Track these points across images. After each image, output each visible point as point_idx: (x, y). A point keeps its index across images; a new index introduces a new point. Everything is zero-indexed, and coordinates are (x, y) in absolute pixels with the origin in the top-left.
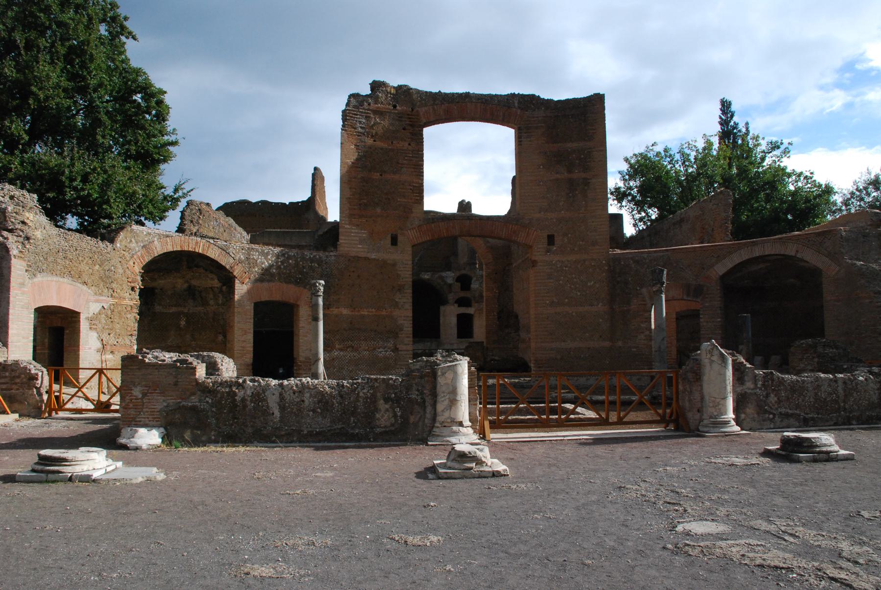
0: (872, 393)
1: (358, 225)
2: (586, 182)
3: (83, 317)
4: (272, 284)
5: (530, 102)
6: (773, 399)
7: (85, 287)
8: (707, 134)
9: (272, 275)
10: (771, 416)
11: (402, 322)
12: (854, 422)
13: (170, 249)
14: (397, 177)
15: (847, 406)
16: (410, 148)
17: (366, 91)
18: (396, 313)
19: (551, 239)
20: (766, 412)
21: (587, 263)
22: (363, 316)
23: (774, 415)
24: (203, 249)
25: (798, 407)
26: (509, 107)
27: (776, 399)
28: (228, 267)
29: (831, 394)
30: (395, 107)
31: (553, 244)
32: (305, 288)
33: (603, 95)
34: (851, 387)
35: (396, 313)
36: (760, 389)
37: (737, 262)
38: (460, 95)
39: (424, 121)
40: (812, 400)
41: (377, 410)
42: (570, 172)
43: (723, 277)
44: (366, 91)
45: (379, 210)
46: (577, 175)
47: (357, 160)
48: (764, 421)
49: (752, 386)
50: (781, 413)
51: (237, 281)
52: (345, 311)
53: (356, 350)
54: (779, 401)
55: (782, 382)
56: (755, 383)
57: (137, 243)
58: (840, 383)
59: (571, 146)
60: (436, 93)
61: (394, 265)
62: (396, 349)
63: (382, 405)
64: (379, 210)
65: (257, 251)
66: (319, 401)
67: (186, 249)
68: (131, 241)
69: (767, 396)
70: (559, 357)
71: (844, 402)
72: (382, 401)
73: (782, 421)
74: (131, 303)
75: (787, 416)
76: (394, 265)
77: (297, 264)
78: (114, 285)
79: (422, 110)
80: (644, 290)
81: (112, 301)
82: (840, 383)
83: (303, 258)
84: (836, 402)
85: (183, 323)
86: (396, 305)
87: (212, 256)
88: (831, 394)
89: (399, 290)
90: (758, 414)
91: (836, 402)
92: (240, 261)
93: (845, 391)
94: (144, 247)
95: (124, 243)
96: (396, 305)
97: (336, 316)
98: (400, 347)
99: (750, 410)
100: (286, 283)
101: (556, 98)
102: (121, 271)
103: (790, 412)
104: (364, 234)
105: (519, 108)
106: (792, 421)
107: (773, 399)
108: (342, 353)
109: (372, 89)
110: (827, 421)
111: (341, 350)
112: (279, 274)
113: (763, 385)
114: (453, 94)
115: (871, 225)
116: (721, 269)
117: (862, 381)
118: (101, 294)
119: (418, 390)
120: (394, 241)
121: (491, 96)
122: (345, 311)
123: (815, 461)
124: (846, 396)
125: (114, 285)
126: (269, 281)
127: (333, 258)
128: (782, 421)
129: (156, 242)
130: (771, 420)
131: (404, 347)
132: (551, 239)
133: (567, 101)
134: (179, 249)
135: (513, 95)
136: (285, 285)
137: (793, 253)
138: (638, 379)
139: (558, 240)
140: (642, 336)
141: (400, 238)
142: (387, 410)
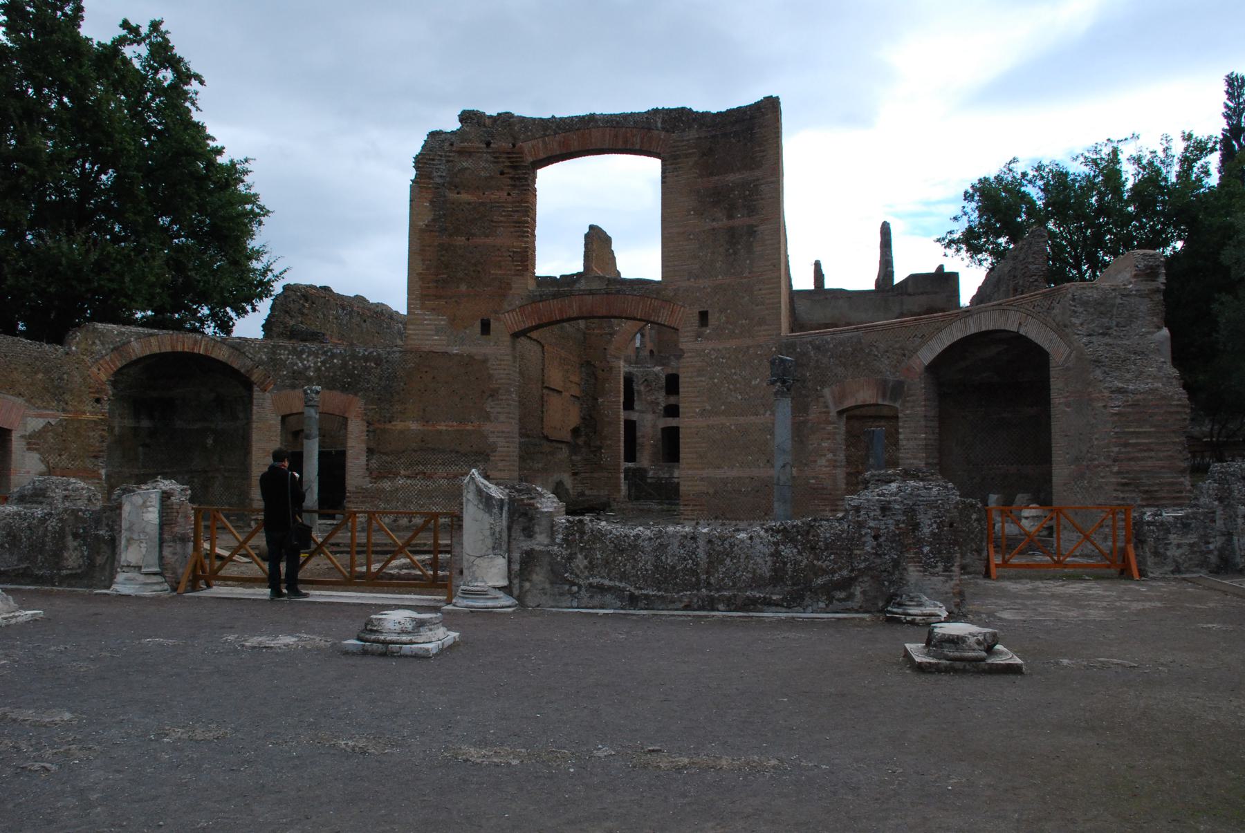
0: (759, 560)
2: (751, 231)
3: (15, 436)
5: (679, 119)
6: (581, 561)
7: (20, 401)
8: (1115, 138)
10: (575, 589)
12: (721, 607)
13: (156, 350)
14: (490, 241)
15: (712, 580)
17: (453, 125)
18: (488, 427)
19: (704, 316)
20: (566, 581)
21: (751, 351)
23: (580, 587)
24: (206, 349)
25: (623, 577)
26: (650, 129)
27: (586, 562)
29: (685, 559)
30: (488, 144)
31: (706, 325)
32: (356, 394)
33: (777, 98)
34: (720, 552)
35: (488, 427)
36: (560, 545)
37: (947, 343)
38: (581, 119)
39: (530, 159)
40: (649, 566)
41: (65, 548)
42: (730, 217)
43: (934, 368)
44: (453, 125)
45: (463, 288)
46: (740, 220)
47: (433, 220)
48: (561, 594)
49: (546, 541)
50: (590, 584)
51: (256, 388)
52: (414, 426)
53: (430, 477)
54: (591, 567)
55: (599, 536)
56: (552, 534)
57: (103, 344)
58: (701, 543)
59: (733, 178)
61: (485, 361)
63: (71, 542)
64: (463, 288)
65: (285, 348)
66: (8, 534)
67: (180, 349)
68: (94, 343)
69: (571, 558)
70: (711, 491)
71: (707, 573)
72: (70, 538)
73: (591, 597)
74: (95, 418)
75: (602, 589)
76: (485, 361)
77: (345, 365)
78: (67, 397)
79: (526, 146)
80: (827, 392)
81: (63, 416)
82: (701, 543)
83: (354, 356)
84: (694, 572)
85: (210, 441)
86: (487, 417)
87: (221, 358)
88: (685, 559)
89: (492, 396)
90: (552, 583)
91: (694, 572)
92: (261, 363)
93: (709, 555)
94: (115, 349)
95: (83, 346)
96: (487, 417)
97: (401, 432)
99: (539, 577)
101: (714, 110)
102: (78, 379)
103: (607, 582)
104: (443, 321)
105: (663, 129)
106: (609, 598)
107: (581, 561)
108: (409, 482)
109: (461, 121)
110: (672, 601)
111: (408, 477)
112: (319, 377)
113: (565, 540)
114: (571, 119)
115: (1135, 276)
116: (927, 355)
117: (742, 541)
118: (45, 408)
119: (107, 525)
120: (486, 327)
121: (625, 117)
122: (414, 426)
123: (365, 653)
124: (710, 563)
125: (67, 397)
127: (398, 354)
128: (591, 597)
129: (134, 344)
130: (573, 595)
132: (704, 316)
133: (730, 112)
134: (169, 349)
135: (656, 111)
137: (1014, 329)
139: (712, 320)
140: (823, 461)
141: (493, 325)
142: (76, 549)
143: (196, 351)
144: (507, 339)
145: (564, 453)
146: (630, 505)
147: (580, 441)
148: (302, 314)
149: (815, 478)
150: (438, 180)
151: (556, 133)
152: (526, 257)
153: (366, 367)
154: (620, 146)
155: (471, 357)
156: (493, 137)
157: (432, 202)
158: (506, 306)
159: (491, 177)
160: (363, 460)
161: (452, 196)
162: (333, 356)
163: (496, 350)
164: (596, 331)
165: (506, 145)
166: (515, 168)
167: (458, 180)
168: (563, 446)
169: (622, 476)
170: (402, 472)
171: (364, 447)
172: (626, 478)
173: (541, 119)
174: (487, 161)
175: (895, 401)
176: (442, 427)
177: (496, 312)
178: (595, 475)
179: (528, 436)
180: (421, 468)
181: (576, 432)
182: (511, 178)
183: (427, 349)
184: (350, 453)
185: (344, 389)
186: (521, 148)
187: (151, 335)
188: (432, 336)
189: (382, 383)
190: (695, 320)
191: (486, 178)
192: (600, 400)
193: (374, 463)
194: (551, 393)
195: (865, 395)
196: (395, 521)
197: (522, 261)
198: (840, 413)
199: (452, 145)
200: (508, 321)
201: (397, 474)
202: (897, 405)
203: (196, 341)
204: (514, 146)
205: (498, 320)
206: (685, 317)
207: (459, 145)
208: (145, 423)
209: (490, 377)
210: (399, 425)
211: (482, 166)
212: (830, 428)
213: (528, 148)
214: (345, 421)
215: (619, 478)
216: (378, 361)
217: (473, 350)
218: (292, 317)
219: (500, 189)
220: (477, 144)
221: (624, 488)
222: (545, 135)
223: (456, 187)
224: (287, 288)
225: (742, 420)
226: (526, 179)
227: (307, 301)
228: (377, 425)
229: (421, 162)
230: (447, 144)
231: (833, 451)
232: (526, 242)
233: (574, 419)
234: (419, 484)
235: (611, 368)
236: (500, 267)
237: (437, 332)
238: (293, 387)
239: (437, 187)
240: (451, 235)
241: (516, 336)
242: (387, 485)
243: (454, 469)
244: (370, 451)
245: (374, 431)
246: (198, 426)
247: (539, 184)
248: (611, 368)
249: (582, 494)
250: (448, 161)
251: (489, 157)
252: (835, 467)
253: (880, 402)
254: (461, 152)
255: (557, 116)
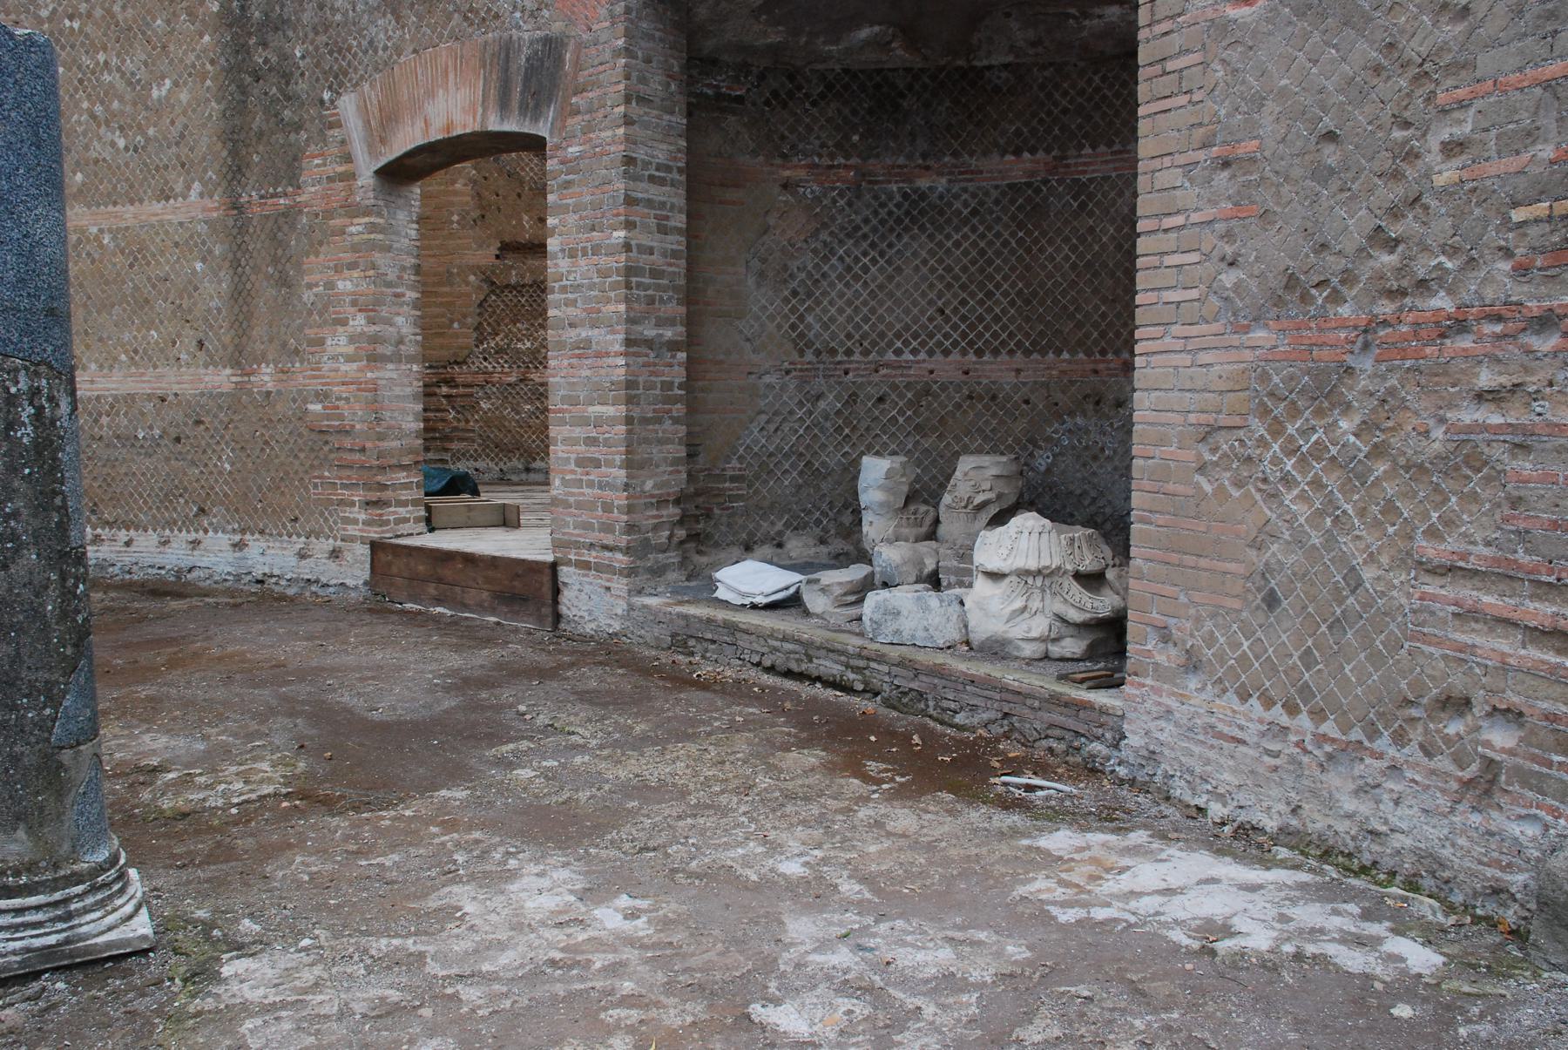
80: (348, 105)
138: (335, 554)
149: (322, 396)
175: (535, 119)
195: (453, 107)
198: (397, 174)
202: (542, 129)
212: (357, 227)
225: (128, 214)
231: (369, 308)
252: (374, 359)
253: (495, 124)
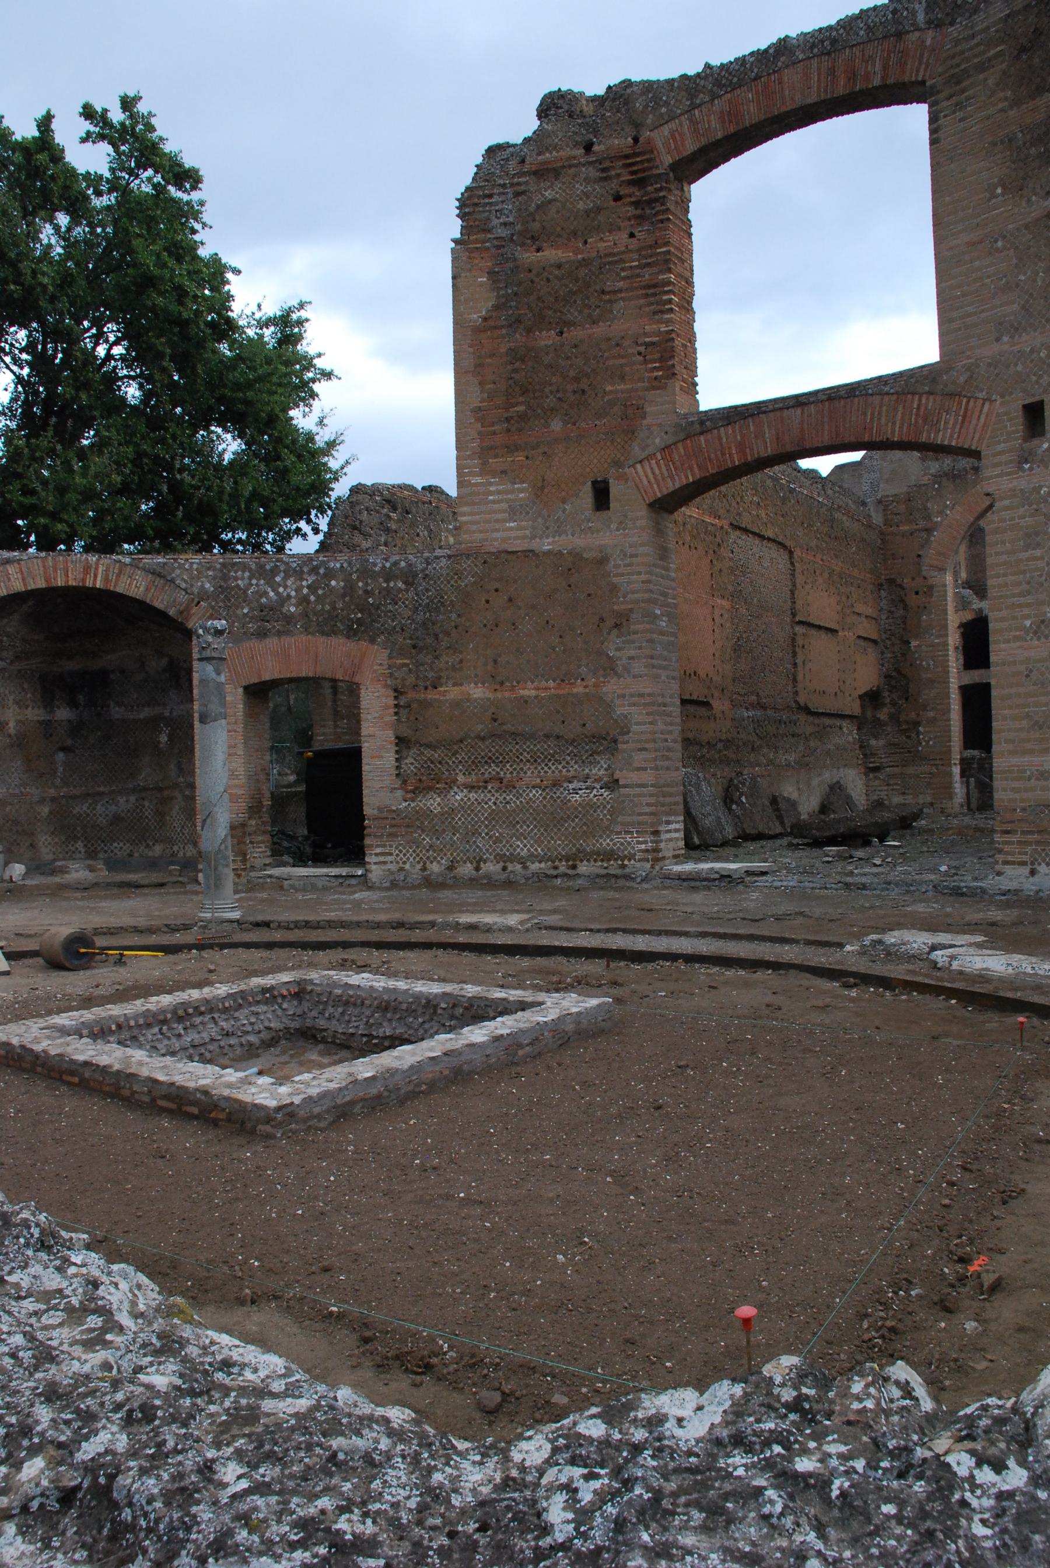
1: (504, 472)
4: (287, 640)
9: (289, 619)
11: (625, 710)
14: (600, 330)
16: (633, 244)
22: (525, 701)
24: (106, 580)
28: (172, 612)
30: (588, 147)
32: (373, 641)
35: (611, 687)
39: (668, 160)
45: (556, 425)
47: (497, 307)
52: (478, 692)
53: (511, 786)
60: (698, 75)
61: (602, 561)
62: (613, 784)
65: (245, 567)
67: (60, 582)
76: (602, 561)
77: (350, 588)
83: (366, 572)
85: (164, 738)
86: (610, 668)
87: (133, 592)
89: (616, 626)
92: (203, 596)
96: (610, 668)
97: (457, 704)
98: (626, 776)
100: (323, 633)
104: (522, 492)
108: (473, 796)
109: (539, 117)
111: (471, 788)
112: (306, 615)
114: (741, 61)
120: (602, 496)
122: (478, 692)
126: (279, 634)
127: (443, 562)
131: (633, 777)
134: (41, 584)
136: (321, 641)
143: (89, 583)
144: (641, 515)
145: (848, 734)
146: (967, 820)
147: (883, 715)
148: (388, 530)
150: (502, 232)
151: (714, 97)
152: (671, 356)
153: (388, 590)
154: (841, 88)
155: (576, 556)
156: (596, 132)
157: (491, 273)
158: (637, 451)
159: (599, 210)
160: (390, 758)
161: (528, 257)
162: (330, 574)
163: (622, 536)
164: (904, 528)
165: (621, 142)
166: (640, 183)
167: (536, 226)
168: (845, 724)
169: (956, 770)
170: (461, 779)
171: (390, 735)
172: (963, 774)
173: (684, 77)
174: (587, 180)
176: (528, 691)
177: (618, 464)
178: (911, 770)
179: (764, 707)
180: (494, 770)
181: (872, 698)
182: (636, 204)
183: (495, 546)
184: (366, 747)
185: (351, 633)
186: (649, 141)
187: (8, 561)
188: (503, 523)
189: (419, 617)
190: (1017, 424)
191: (587, 213)
192: (914, 643)
193: (410, 764)
194: (813, 632)
196: (450, 868)
197: (661, 360)
199: (523, 161)
200: (643, 479)
201: (451, 783)
203: (87, 568)
204: (636, 140)
205: (623, 478)
206: (995, 427)
207: (533, 160)
208: (63, 714)
209: (614, 588)
210: (451, 692)
211: (578, 192)
213: (667, 143)
214: (354, 690)
215: (950, 775)
216: (410, 577)
217: (579, 542)
218: (366, 536)
219: (614, 228)
220: (568, 152)
221: (959, 789)
222: (693, 107)
223: (535, 240)
224: (356, 490)
226: (662, 201)
227: (394, 509)
228: (411, 695)
229: (472, 205)
230: (512, 164)
232: (669, 321)
233: (867, 674)
234: (491, 799)
235: (931, 588)
236: (622, 378)
237: (513, 513)
238: (262, 634)
239: (501, 244)
240: (529, 331)
241: (666, 505)
242: (433, 803)
243: (553, 770)
244: (402, 742)
245: (408, 706)
246: (146, 713)
247: (696, 213)
248: (931, 588)
249: (879, 804)
250: (517, 194)
251: (592, 172)
254: (542, 173)
255: (716, 62)
